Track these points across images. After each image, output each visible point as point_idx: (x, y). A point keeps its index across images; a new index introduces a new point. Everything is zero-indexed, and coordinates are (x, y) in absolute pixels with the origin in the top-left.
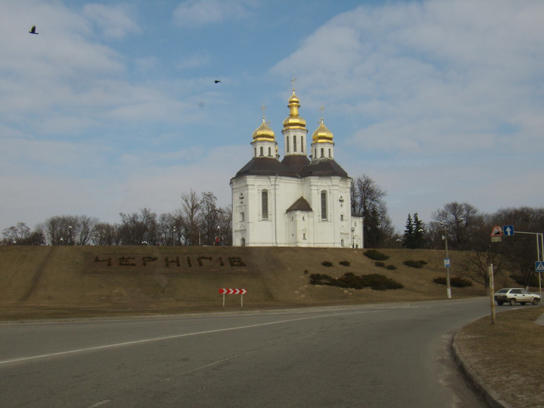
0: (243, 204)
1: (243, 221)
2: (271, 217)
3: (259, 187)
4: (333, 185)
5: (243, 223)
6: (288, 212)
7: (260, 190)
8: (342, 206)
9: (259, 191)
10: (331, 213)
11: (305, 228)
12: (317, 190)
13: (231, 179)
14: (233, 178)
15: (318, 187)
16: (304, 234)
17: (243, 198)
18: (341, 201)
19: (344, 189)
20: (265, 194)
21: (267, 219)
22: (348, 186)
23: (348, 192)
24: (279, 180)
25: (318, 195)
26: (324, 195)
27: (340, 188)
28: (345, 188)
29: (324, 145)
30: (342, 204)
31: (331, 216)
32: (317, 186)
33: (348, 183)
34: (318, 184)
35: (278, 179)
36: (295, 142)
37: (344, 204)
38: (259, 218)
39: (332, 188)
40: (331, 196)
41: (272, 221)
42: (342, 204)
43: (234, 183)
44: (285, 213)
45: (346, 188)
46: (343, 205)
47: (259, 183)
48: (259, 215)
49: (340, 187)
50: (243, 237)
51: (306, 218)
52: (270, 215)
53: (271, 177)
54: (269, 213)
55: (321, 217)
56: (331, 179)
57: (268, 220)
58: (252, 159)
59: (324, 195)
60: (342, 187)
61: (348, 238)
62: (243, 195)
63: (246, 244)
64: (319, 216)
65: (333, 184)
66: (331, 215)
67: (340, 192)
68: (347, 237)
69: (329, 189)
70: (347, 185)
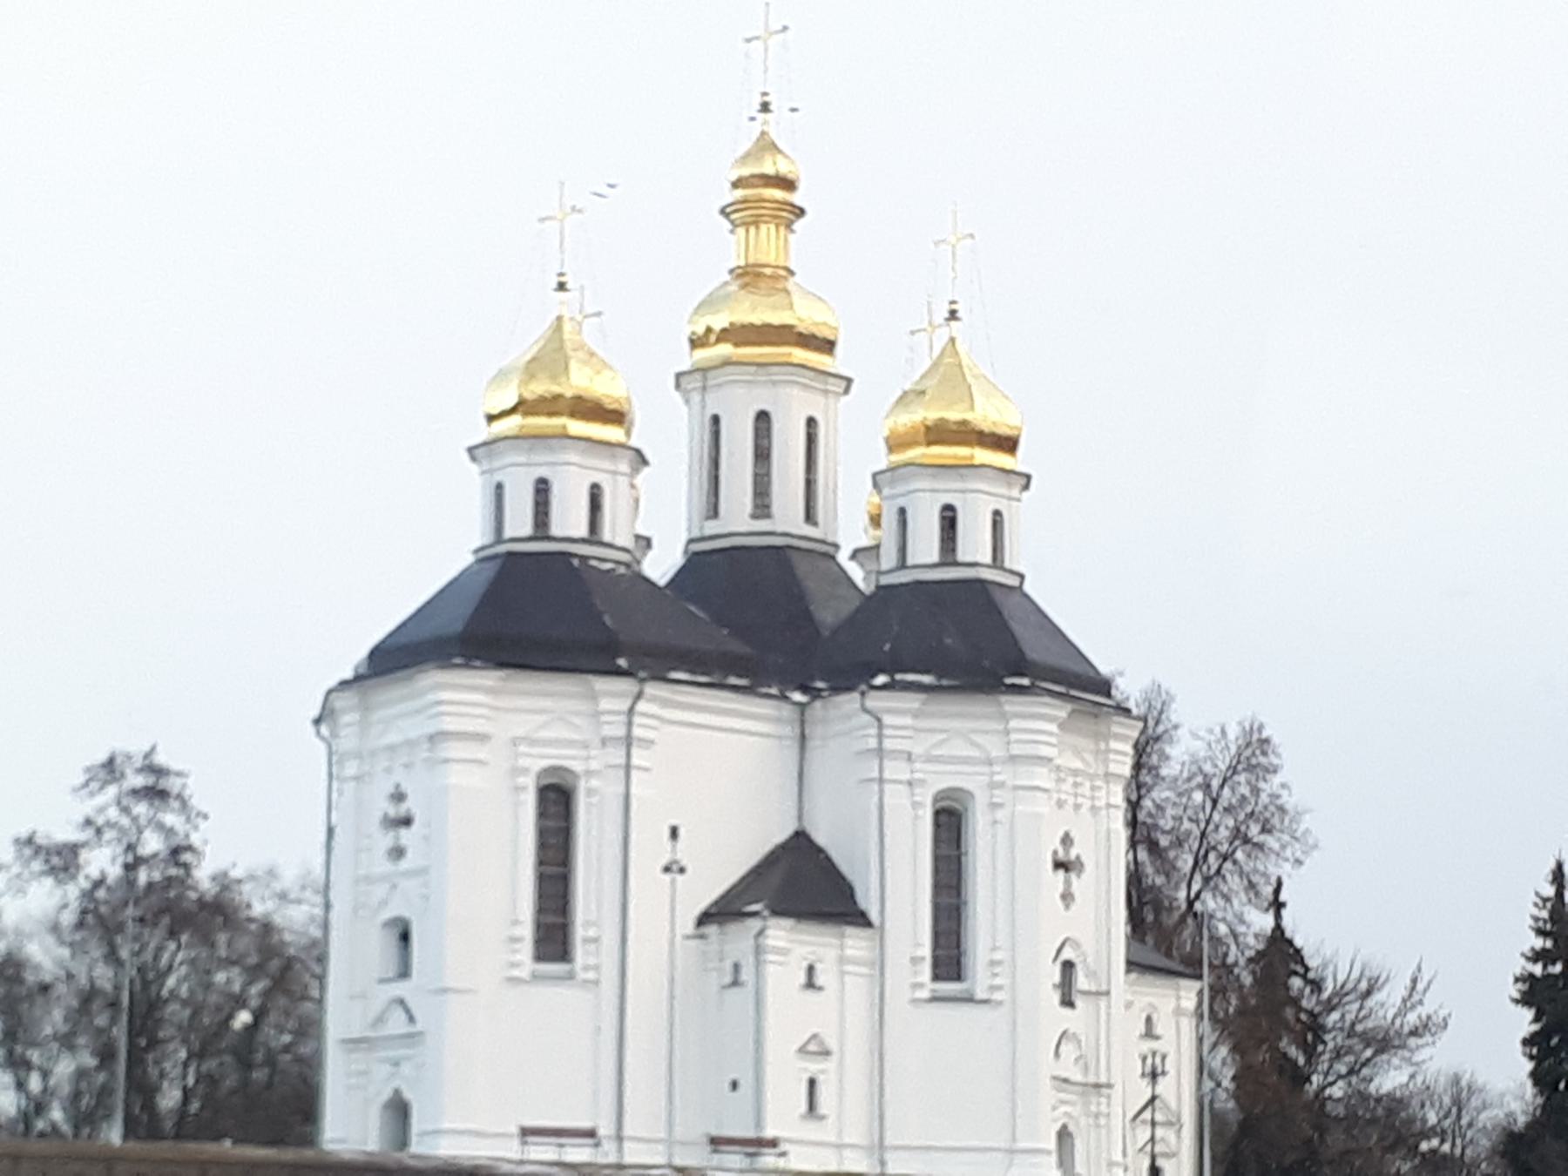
0: (405, 864)
1: (404, 972)
2: (592, 961)
3: (522, 748)
4: (1013, 759)
5: (400, 989)
6: (712, 930)
7: (525, 771)
8: (1067, 897)
9: (521, 780)
10: (994, 949)
12: (910, 783)
13: (330, 692)
14: (344, 684)
15: (918, 766)
16: (812, 1083)
17: (407, 821)
18: (1059, 865)
19: (1086, 789)
22: (1113, 768)
23: (1109, 806)
25: (916, 817)
27: (1059, 780)
28: (1092, 777)
29: (959, 485)
30: (1068, 883)
31: (993, 963)
32: (909, 757)
33: (1114, 745)
34: (918, 750)
35: (653, 699)
36: (762, 454)
37: (1080, 885)
38: (514, 965)
39: (1004, 774)
40: (1002, 831)
41: (596, 983)
42: (1068, 883)
43: (346, 718)
45: (1098, 783)
47: (521, 725)
48: (515, 940)
49: (1058, 768)
50: (397, 1092)
52: (586, 940)
53: (601, 684)
55: (926, 970)
56: (1004, 717)
57: (570, 976)
58: (469, 559)
60: (1075, 773)
61: (1102, 1121)
62: (411, 805)
63: (414, 1139)
64: (915, 961)
65: (1016, 750)
66: (998, 956)
67: (1060, 804)
68: (1093, 1108)
69: (986, 779)
70: (1106, 761)
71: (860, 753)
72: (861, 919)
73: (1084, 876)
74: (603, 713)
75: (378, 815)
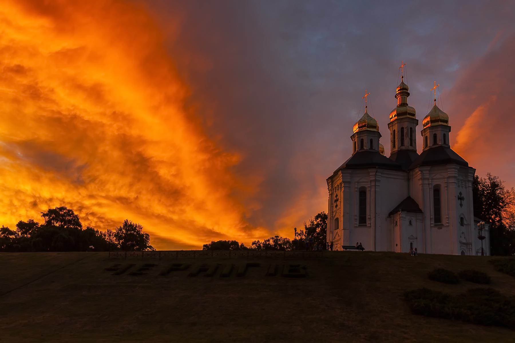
2: (369, 222)
8: (461, 205)
11: (412, 235)
15: (430, 181)
20: (363, 193)
21: (365, 224)
22: (469, 179)
23: (469, 187)
24: (380, 174)
26: (437, 191)
30: (461, 202)
33: (469, 174)
37: (464, 202)
38: (356, 224)
42: (461, 202)
44: (387, 217)
46: (463, 203)
50: (337, 249)
51: (413, 223)
53: (370, 170)
54: (367, 217)
59: (437, 191)
67: (459, 186)
71: (419, 180)
72: (420, 211)
73: (464, 201)
74: (371, 175)
75: (334, 200)
